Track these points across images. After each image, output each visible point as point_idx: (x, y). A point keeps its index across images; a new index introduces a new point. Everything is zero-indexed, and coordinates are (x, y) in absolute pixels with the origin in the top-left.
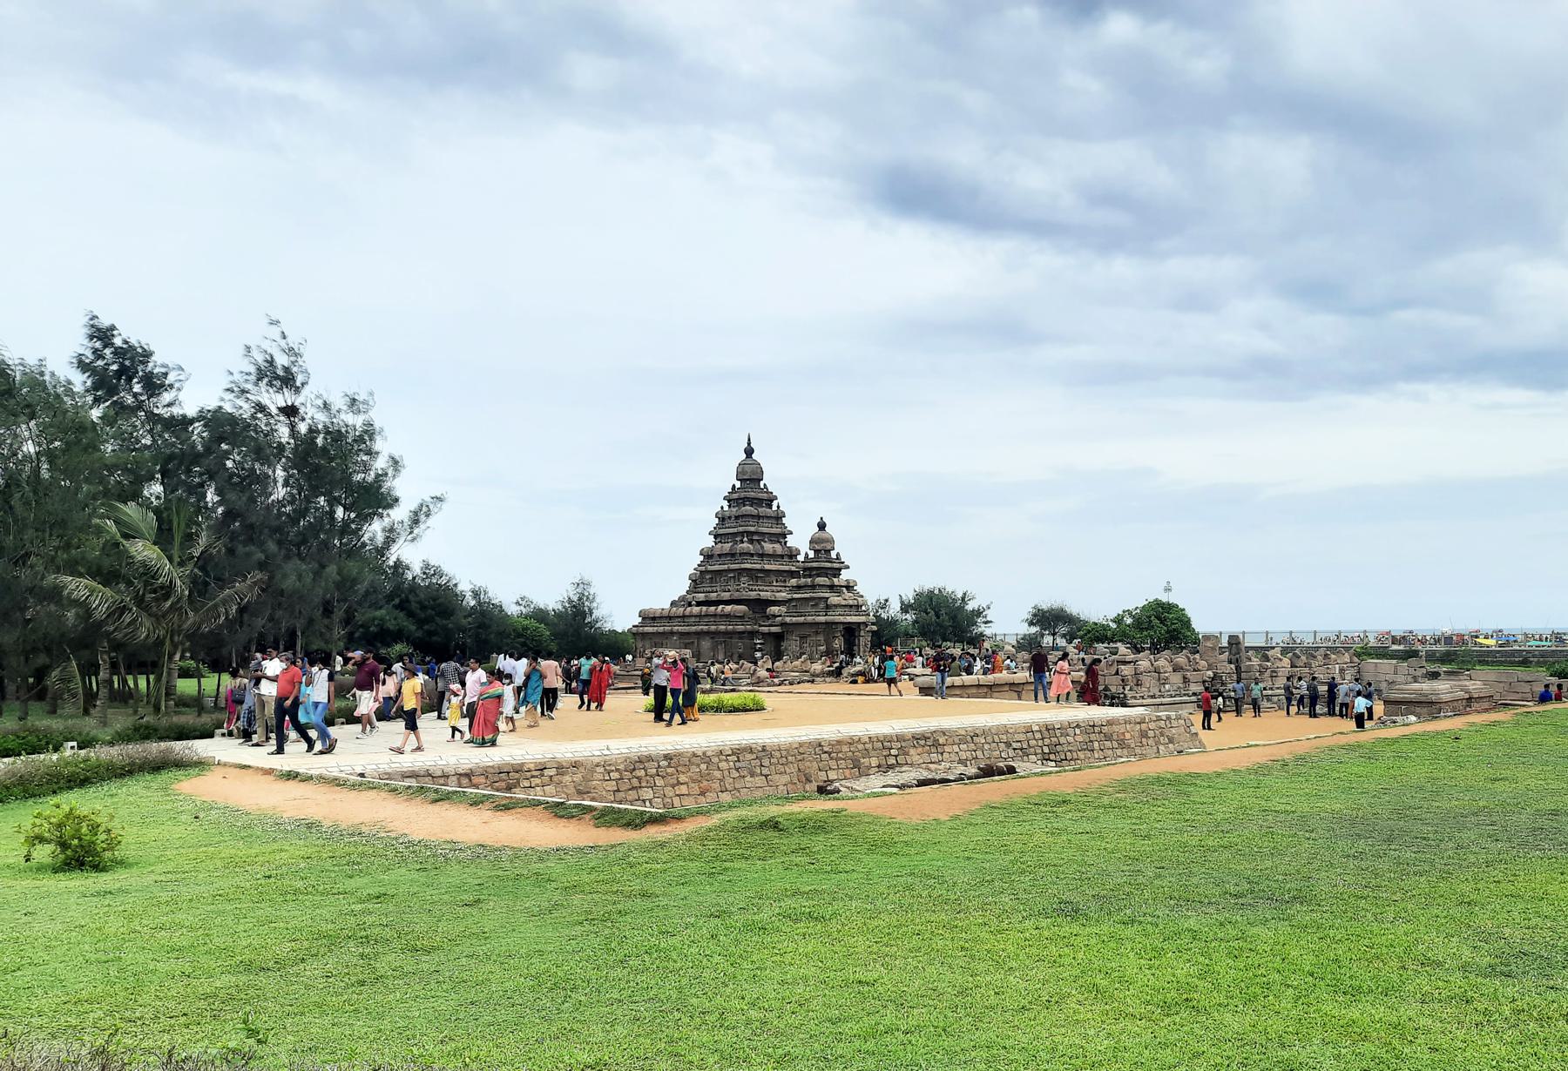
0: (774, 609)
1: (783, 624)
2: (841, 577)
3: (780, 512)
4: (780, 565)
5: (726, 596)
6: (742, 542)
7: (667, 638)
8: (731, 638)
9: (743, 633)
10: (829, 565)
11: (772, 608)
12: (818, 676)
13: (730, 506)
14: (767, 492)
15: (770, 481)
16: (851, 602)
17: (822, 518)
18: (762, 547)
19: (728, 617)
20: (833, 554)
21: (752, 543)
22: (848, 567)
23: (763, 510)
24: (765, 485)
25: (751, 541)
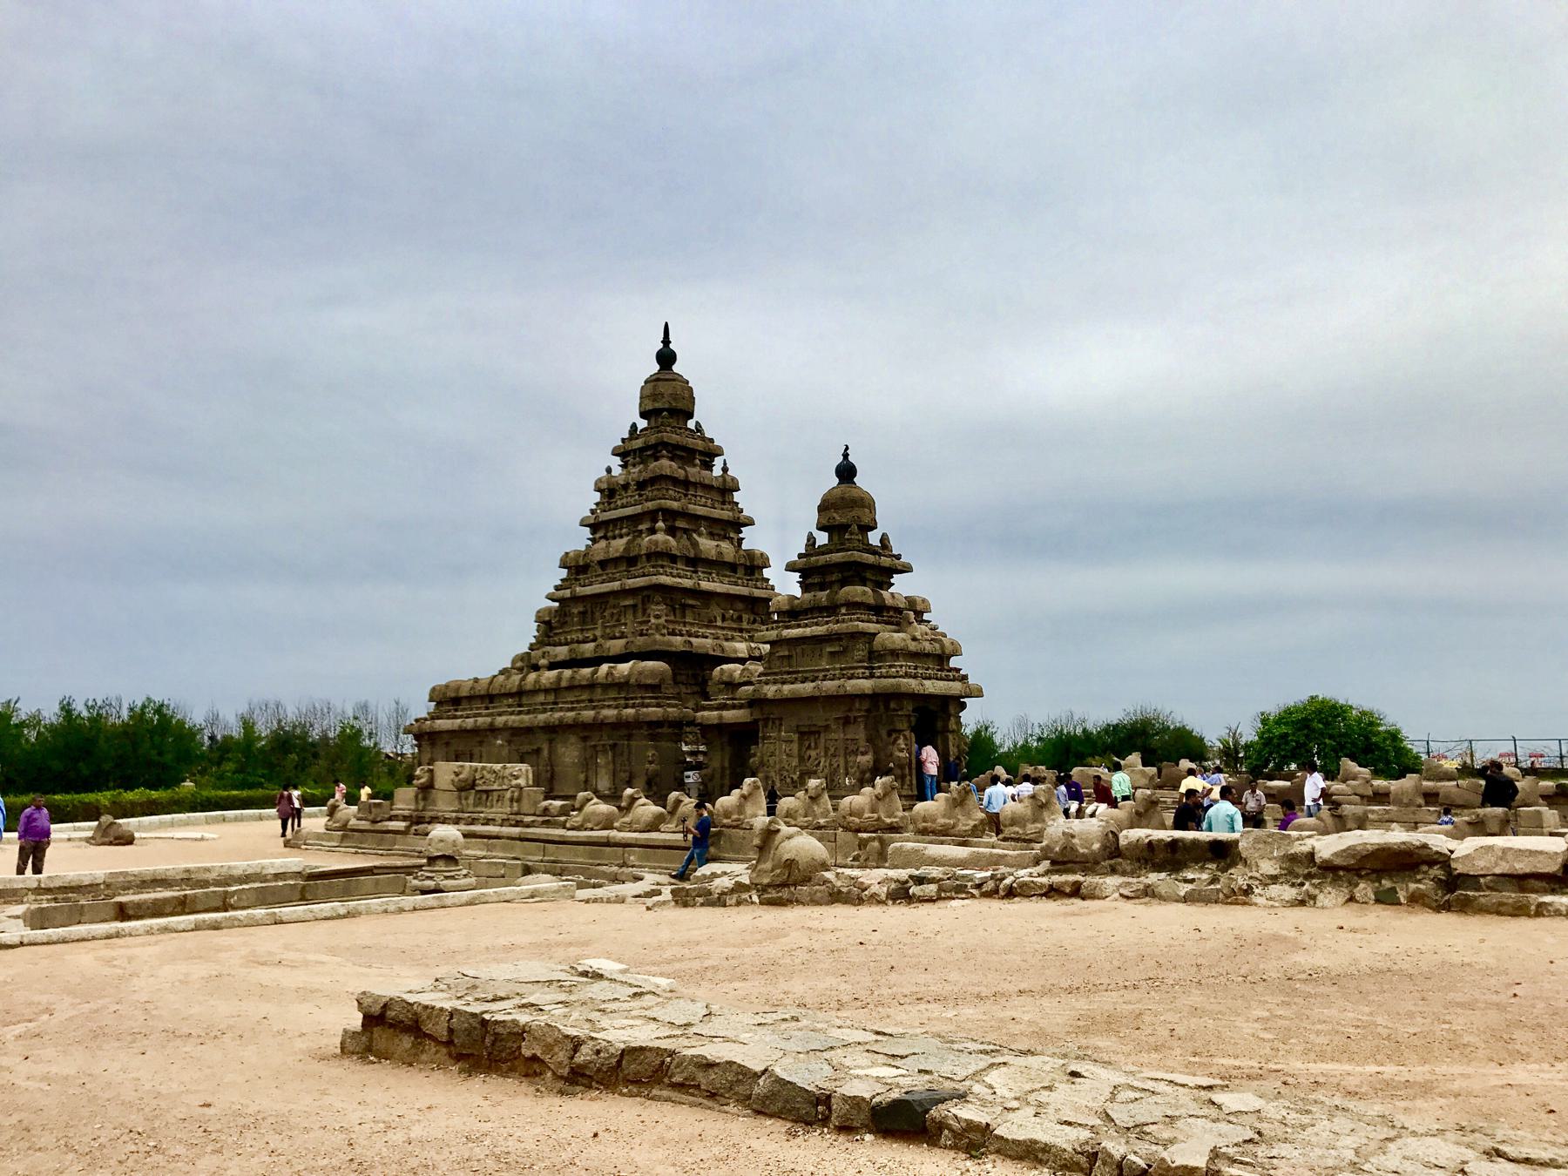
0: (736, 668)
1: (755, 703)
3: (728, 479)
4: (730, 583)
5: (616, 646)
6: (653, 531)
7: (481, 743)
8: (629, 737)
9: (658, 724)
10: (869, 558)
11: (725, 667)
12: (1088, 864)
13: (624, 466)
14: (703, 438)
15: (709, 416)
16: (927, 647)
18: (695, 545)
19: (621, 686)
20: (874, 538)
21: (674, 537)
23: (694, 472)
24: (697, 423)
25: (671, 531)
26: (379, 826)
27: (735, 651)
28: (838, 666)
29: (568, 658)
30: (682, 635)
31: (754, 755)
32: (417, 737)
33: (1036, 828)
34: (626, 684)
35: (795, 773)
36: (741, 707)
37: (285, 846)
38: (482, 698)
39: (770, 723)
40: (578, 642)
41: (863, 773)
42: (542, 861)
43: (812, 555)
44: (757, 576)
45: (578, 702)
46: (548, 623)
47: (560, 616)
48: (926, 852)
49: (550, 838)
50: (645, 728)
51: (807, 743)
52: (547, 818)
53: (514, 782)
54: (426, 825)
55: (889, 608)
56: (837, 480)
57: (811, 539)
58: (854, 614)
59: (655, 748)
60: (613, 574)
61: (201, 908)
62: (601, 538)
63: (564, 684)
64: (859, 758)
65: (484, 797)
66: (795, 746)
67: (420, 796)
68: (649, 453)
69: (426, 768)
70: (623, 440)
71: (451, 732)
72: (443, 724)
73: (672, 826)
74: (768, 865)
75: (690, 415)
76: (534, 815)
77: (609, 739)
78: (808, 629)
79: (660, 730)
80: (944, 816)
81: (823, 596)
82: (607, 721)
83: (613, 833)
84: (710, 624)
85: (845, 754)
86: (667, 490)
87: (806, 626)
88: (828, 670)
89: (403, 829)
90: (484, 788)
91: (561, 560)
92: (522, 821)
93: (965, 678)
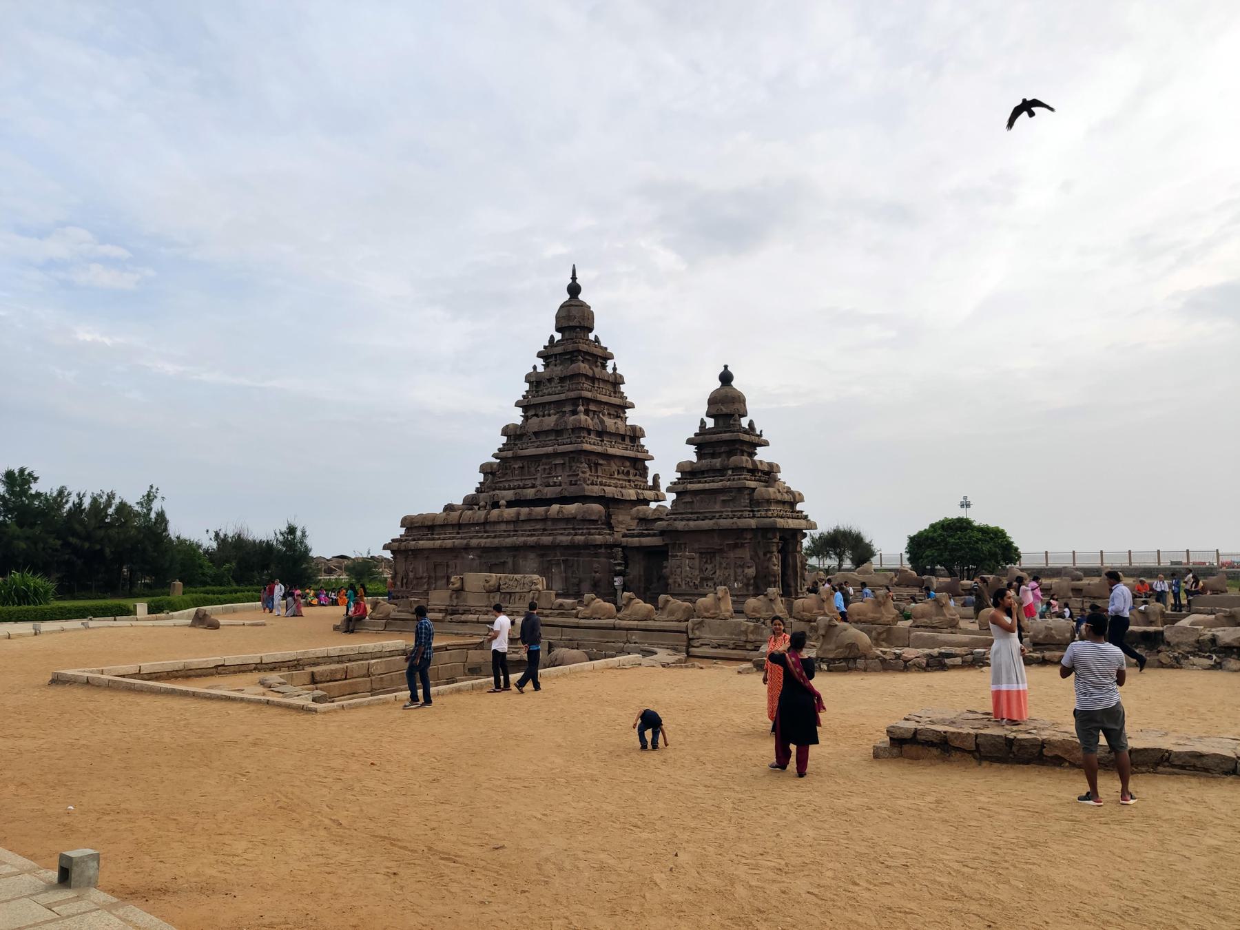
2: (756, 458)
6: (575, 412)
7: (456, 557)
8: (578, 555)
9: (600, 546)
10: (746, 437)
13: (546, 366)
14: (601, 347)
15: (604, 331)
17: (726, 367)
18: (602, 422)
20: (744, 422)
21: (588, 416)
22: (766, 444)
24: (596, 336)
25: (587, 412)
27: (629, 495)
28: (729, 509)
29: (514, 499)
30: (597, 485)
31: (666, 567)
32: (393, 552)
33: (940, 619)
34: (575, 518)
35: (696, 580)
36: (654, 535)
37: (334, 630)
38: (453, 525)
39: (677, 546)
40: (518, 488)
41: (749, 579)
43: (706, 434)
44: (637, 443)
45: (534, 530)
46: (493, 474)
47: (503, 469)
48: (939, 638)
50: (592, 549)
51: (705, 560)
53: (533, 587)
54: (460, 616)
55: (759, 471)
56: (720, 384)
57: (702, 422)
58: (740, 475)
59: (599, 563)
60: (545, 441)
61: (356, 676)
62: (533, 416)
63: (522, 518)
64: (746, 571)
65: (508, 597)
66: (697, 562)
67: (454, 596)
68: (567, 357)
69: (458, 577)
70: (545, 347)
71: (433, 550)
72: (423, 544)
73: (664, 617)
74: (832, 646)
75: (591, 330)
76: (551, 609)
77: (562, 556)
78: (707, 484)
79: (599, 551)
80: (872, 613)
81: (717, 462)
82: (561, 544)
83: (617, 622)
84: (611, 476)
85: (735, 567)
86: (583, 383)
87: (706, 482)
88: (722, 512)
89: (441, 618)
90: (508, 590)
91: (503, 430)
92: (542, 613)
93: (806, 517)
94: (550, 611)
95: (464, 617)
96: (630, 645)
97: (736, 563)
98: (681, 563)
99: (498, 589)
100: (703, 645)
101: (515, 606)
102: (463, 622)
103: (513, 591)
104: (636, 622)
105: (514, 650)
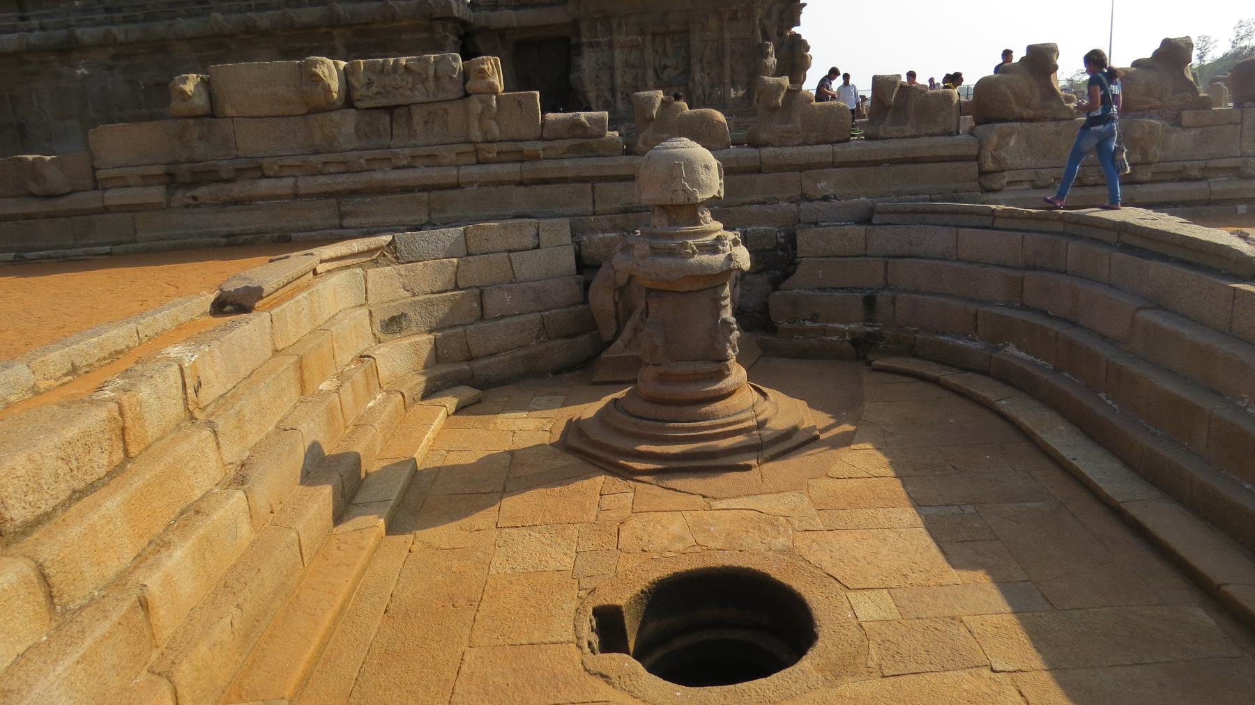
26: (63, 204)
42: (594, 214)
49: (607, 172)
52: (578, 141)
54: (221, 186)
65: (387, 119)
76: (541, 138)
90: (383, 102)
92: (521, 151)
94: (539, 146)
95: (238, 189)
96: (816, 205)
97: (733, 52)
98: (612, 58)
99: (348, 101)
100: (1009, 183)
101: (413, 142)
102: (236, 202)
103: (400, 101)
104: (826, 148)
105: (700, 241)
